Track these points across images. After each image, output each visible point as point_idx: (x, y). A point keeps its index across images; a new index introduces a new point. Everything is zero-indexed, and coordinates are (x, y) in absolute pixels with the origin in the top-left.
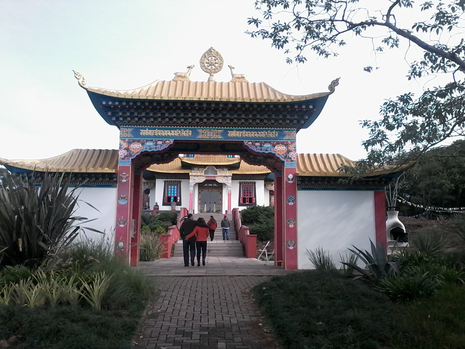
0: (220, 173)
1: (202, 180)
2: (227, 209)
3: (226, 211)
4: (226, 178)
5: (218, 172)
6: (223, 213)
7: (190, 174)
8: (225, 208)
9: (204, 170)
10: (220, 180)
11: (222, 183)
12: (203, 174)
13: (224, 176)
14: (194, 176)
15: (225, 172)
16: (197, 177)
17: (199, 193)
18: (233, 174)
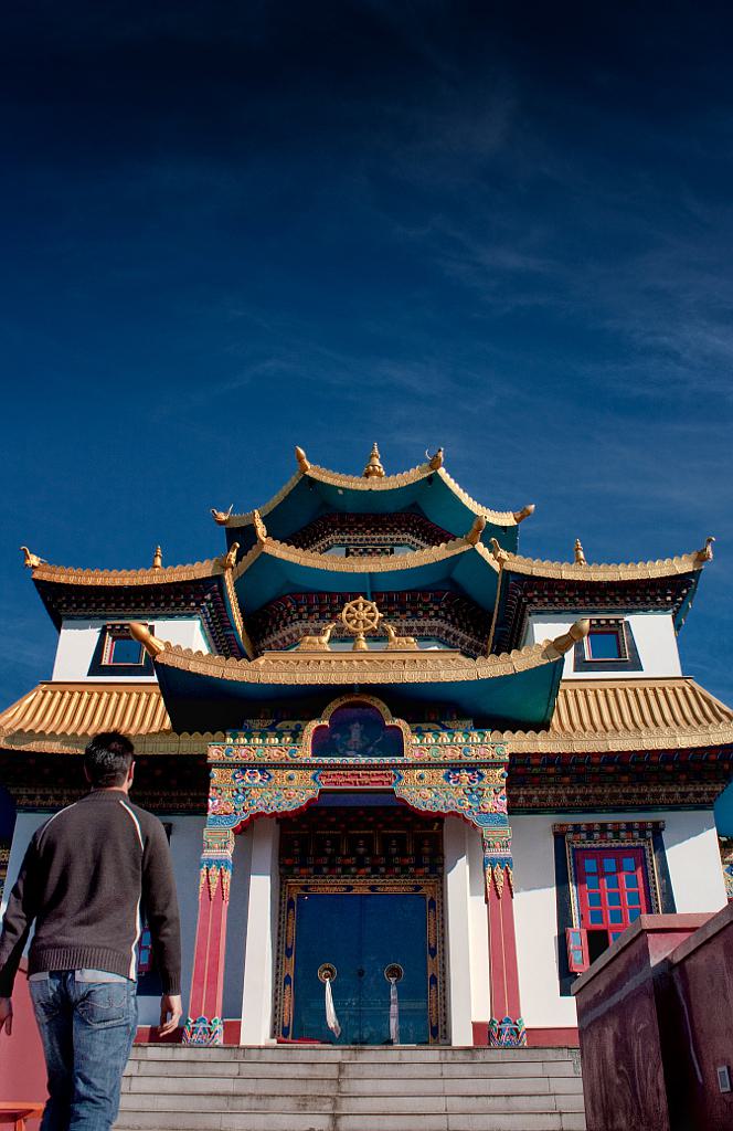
0: (417, 745)
1: (295, 792)
2: (484, 1016)
3: (478, 1028)
4: (465, 775)
5: (411, 740)
6: (456, 1043)
7: (214, 753)
8: (470, 1001)
9: (314, 724)
10: (422, 792)
11: (439, 818)
12: (305, 753)
13: (455, 767)
14: (243, 767)
15: (461, 739)
16: (269, 775)
17: (284, 906)
18: (511, 755)
